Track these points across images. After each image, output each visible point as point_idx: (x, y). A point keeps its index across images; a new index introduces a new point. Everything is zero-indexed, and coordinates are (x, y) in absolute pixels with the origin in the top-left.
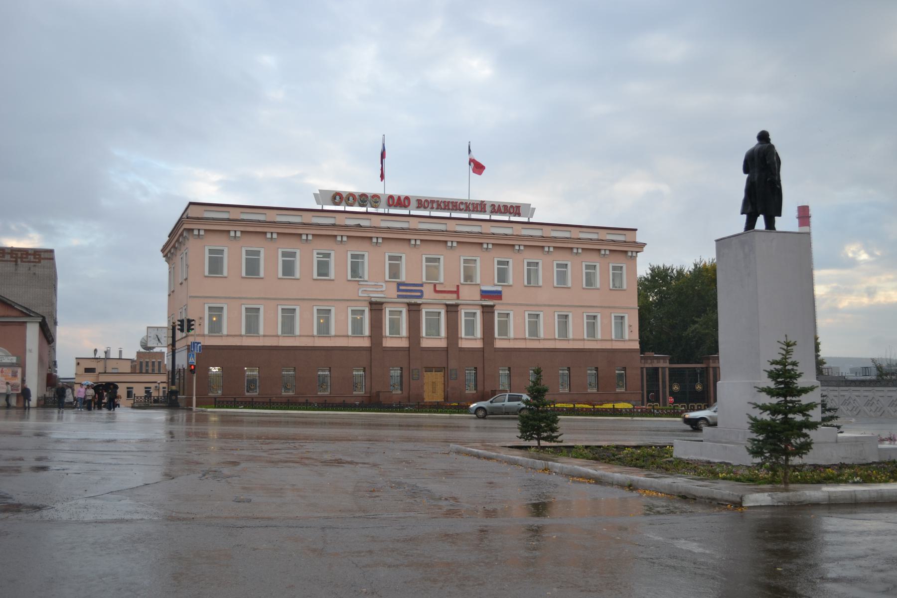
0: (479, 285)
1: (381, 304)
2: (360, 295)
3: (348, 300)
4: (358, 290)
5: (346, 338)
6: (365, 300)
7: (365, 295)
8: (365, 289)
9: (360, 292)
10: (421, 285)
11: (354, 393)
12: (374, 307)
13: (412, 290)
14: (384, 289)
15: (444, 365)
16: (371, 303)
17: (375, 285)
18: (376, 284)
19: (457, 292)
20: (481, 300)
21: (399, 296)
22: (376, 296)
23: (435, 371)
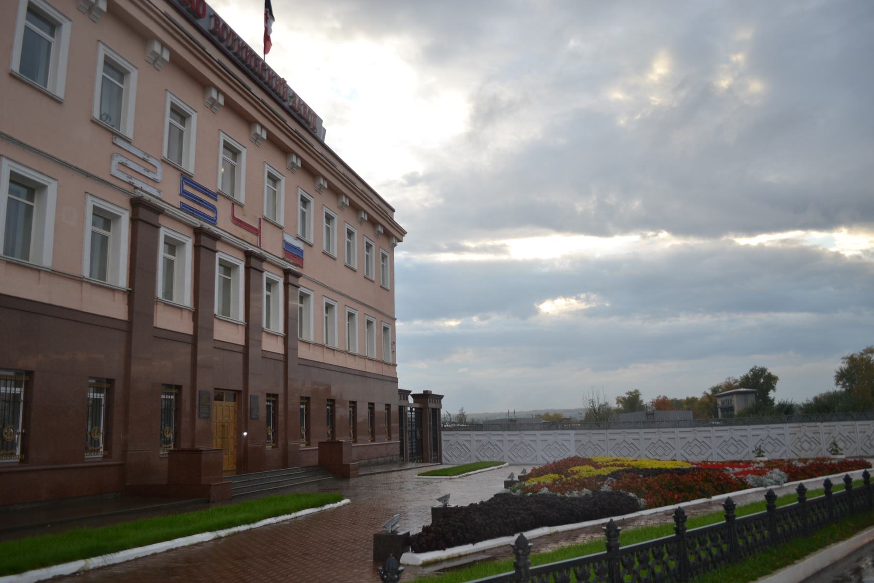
0: (281, 228)
1: (159, 211)
2: (114, 171)
3: (88, 175)
4: (112, 157)
5: (75, 286)
6: (124, 192)
7: (124, 178)
8: (124, 160)
9: (115, 162)
10: (214, 196)
11: (88, 456)
12: (143, 214)
13: (202, 200)
14: (158, 177)
15: (239, 386)
16: (137, 204)
17: (144, 160)
18: (146, 157)
19: (257, 232)
20: (283, 259)
21: (184, 208)
22: (148, 190)
23: (226, 401)
